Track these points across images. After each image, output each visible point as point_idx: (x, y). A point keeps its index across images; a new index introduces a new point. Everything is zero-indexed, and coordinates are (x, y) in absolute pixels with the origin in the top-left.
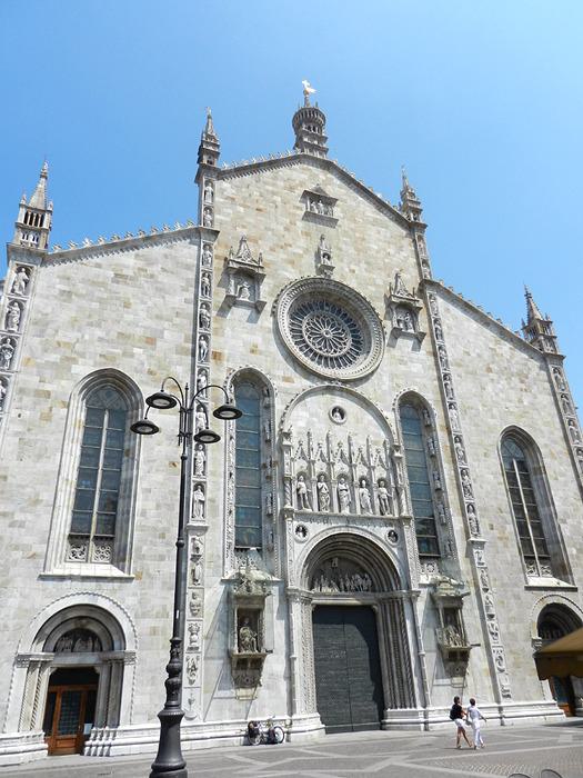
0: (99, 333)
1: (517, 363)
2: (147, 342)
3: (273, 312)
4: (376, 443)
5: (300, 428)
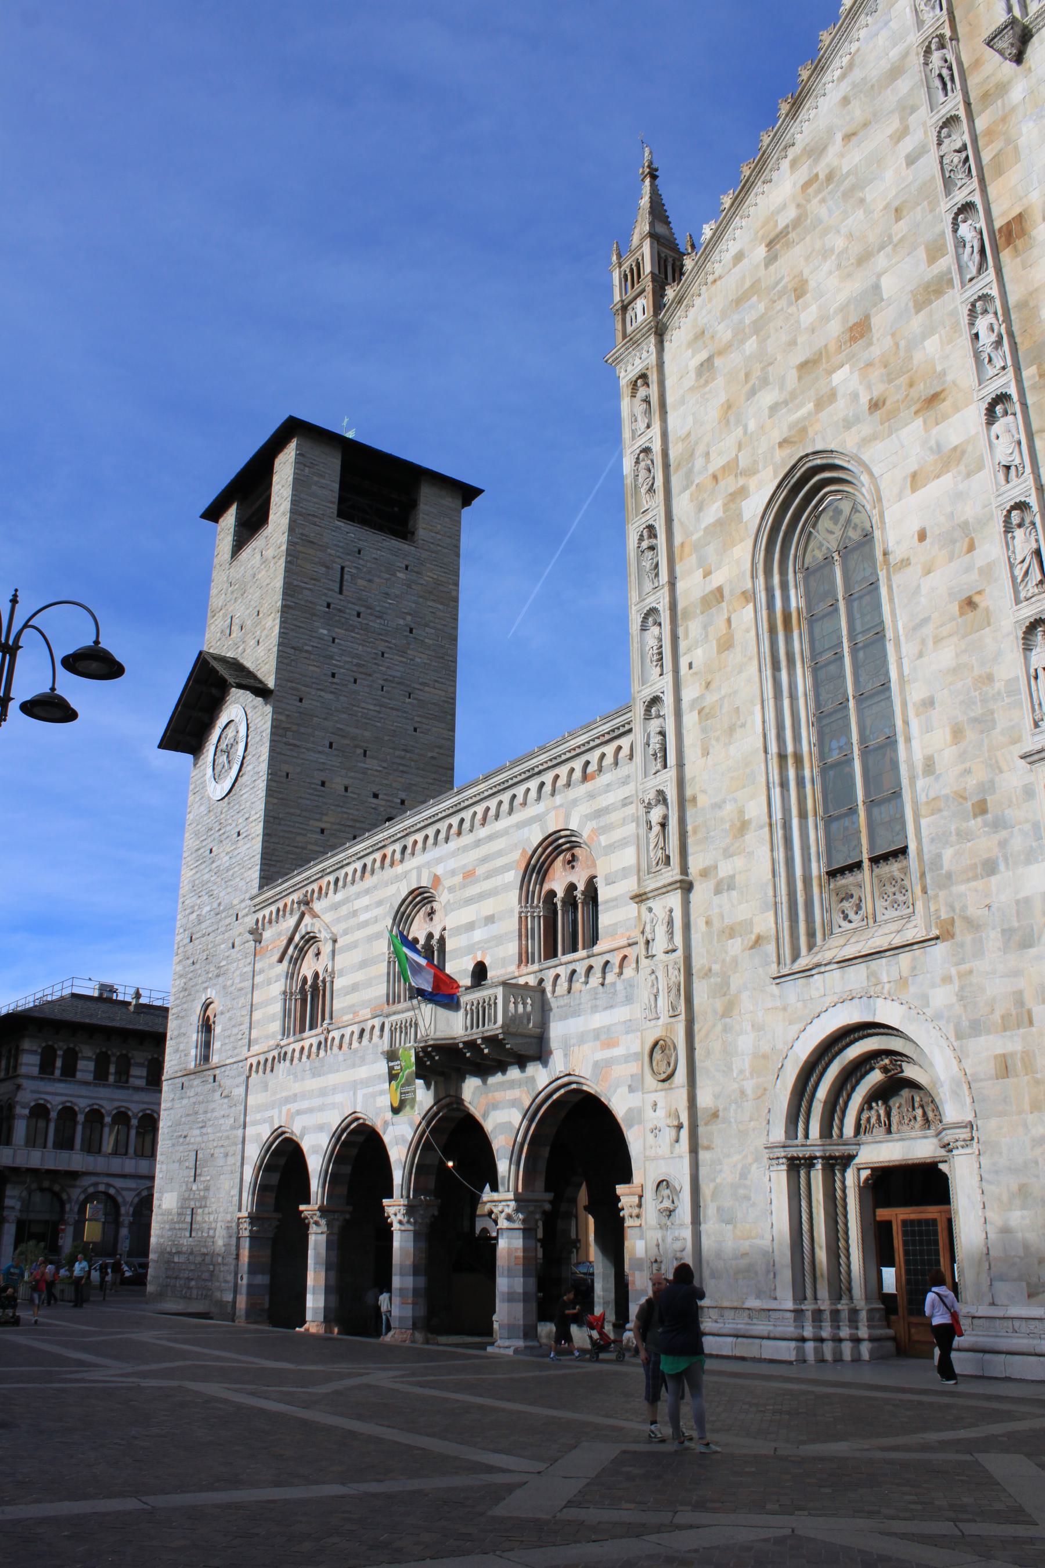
0: (767, 398)
2: (853, 339)
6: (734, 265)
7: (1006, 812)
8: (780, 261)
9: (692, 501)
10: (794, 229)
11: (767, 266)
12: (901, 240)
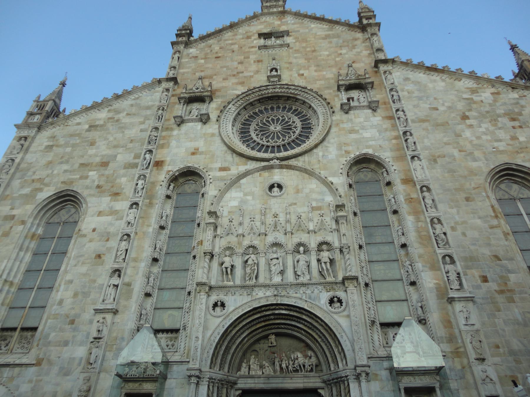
0: (65, 167)
1: (505, 104)
2: (101, 166)
3: (217, 120)
4: (319, 208)
5: (231, 207)
6: (76, 125)
8: (91, 133)
9: (20, 184)
10: (100, 127)
12: (129, 148)
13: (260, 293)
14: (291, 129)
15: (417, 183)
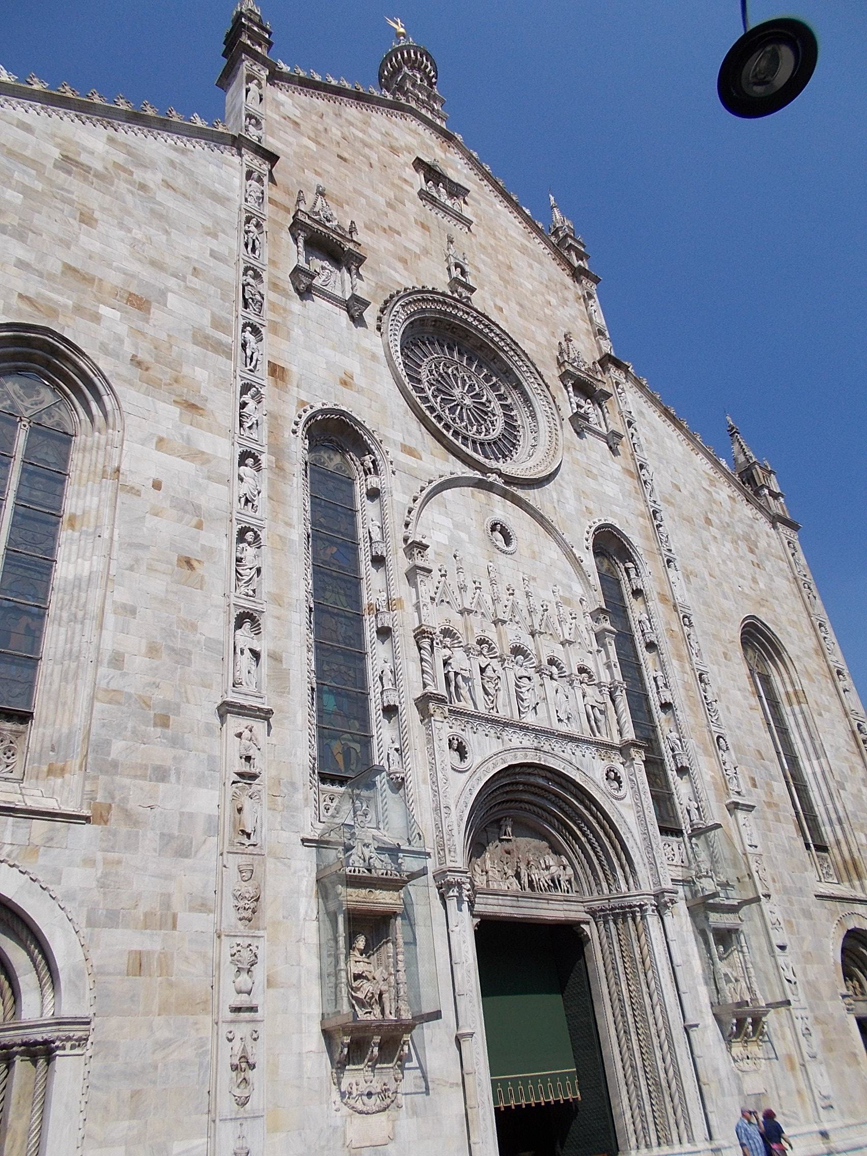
4: (567, 602)
6: (18, 126)
7: (186, 735)
10: (96, 176)
11: (55, 166)
13: (516, 739)
14: (486, 414)
15: (679, 609)
